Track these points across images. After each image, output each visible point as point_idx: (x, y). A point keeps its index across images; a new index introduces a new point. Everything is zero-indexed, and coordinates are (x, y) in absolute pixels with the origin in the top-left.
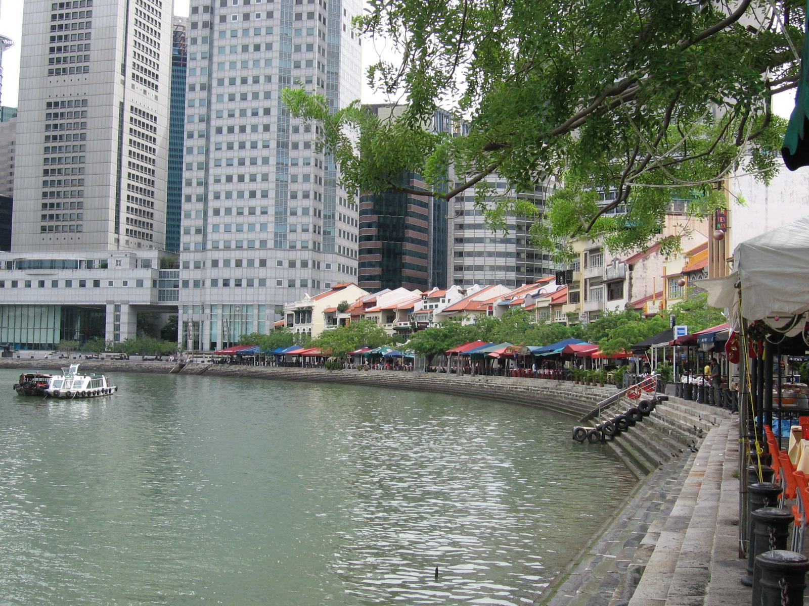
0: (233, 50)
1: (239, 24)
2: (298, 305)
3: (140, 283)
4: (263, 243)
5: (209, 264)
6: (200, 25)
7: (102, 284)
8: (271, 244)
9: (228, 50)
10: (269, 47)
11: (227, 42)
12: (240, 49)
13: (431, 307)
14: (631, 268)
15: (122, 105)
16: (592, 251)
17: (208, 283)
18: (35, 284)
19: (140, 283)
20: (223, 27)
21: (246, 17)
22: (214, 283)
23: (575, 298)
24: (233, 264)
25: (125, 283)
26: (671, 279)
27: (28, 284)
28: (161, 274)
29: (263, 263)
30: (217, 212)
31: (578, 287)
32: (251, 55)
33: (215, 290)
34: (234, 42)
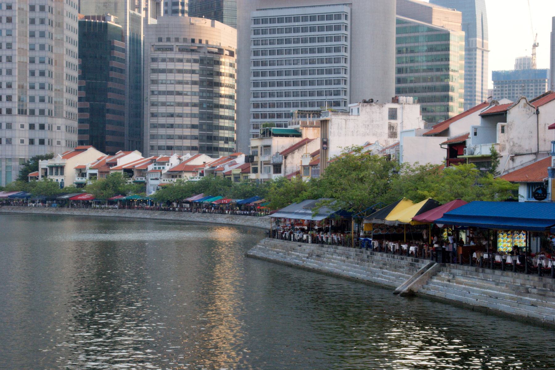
2: (50, 162)
4: (9, 111)
8: (15, 111)
13: (159, 168)
14: (286, 158)
16: (265, 146)
23: (255, 171)
26: (304, 167)
31: (257, 164)
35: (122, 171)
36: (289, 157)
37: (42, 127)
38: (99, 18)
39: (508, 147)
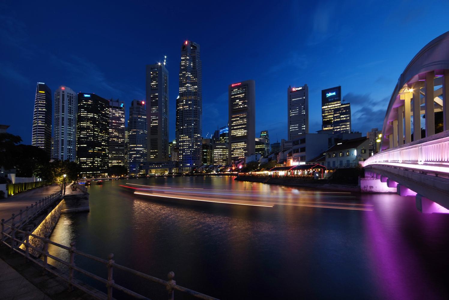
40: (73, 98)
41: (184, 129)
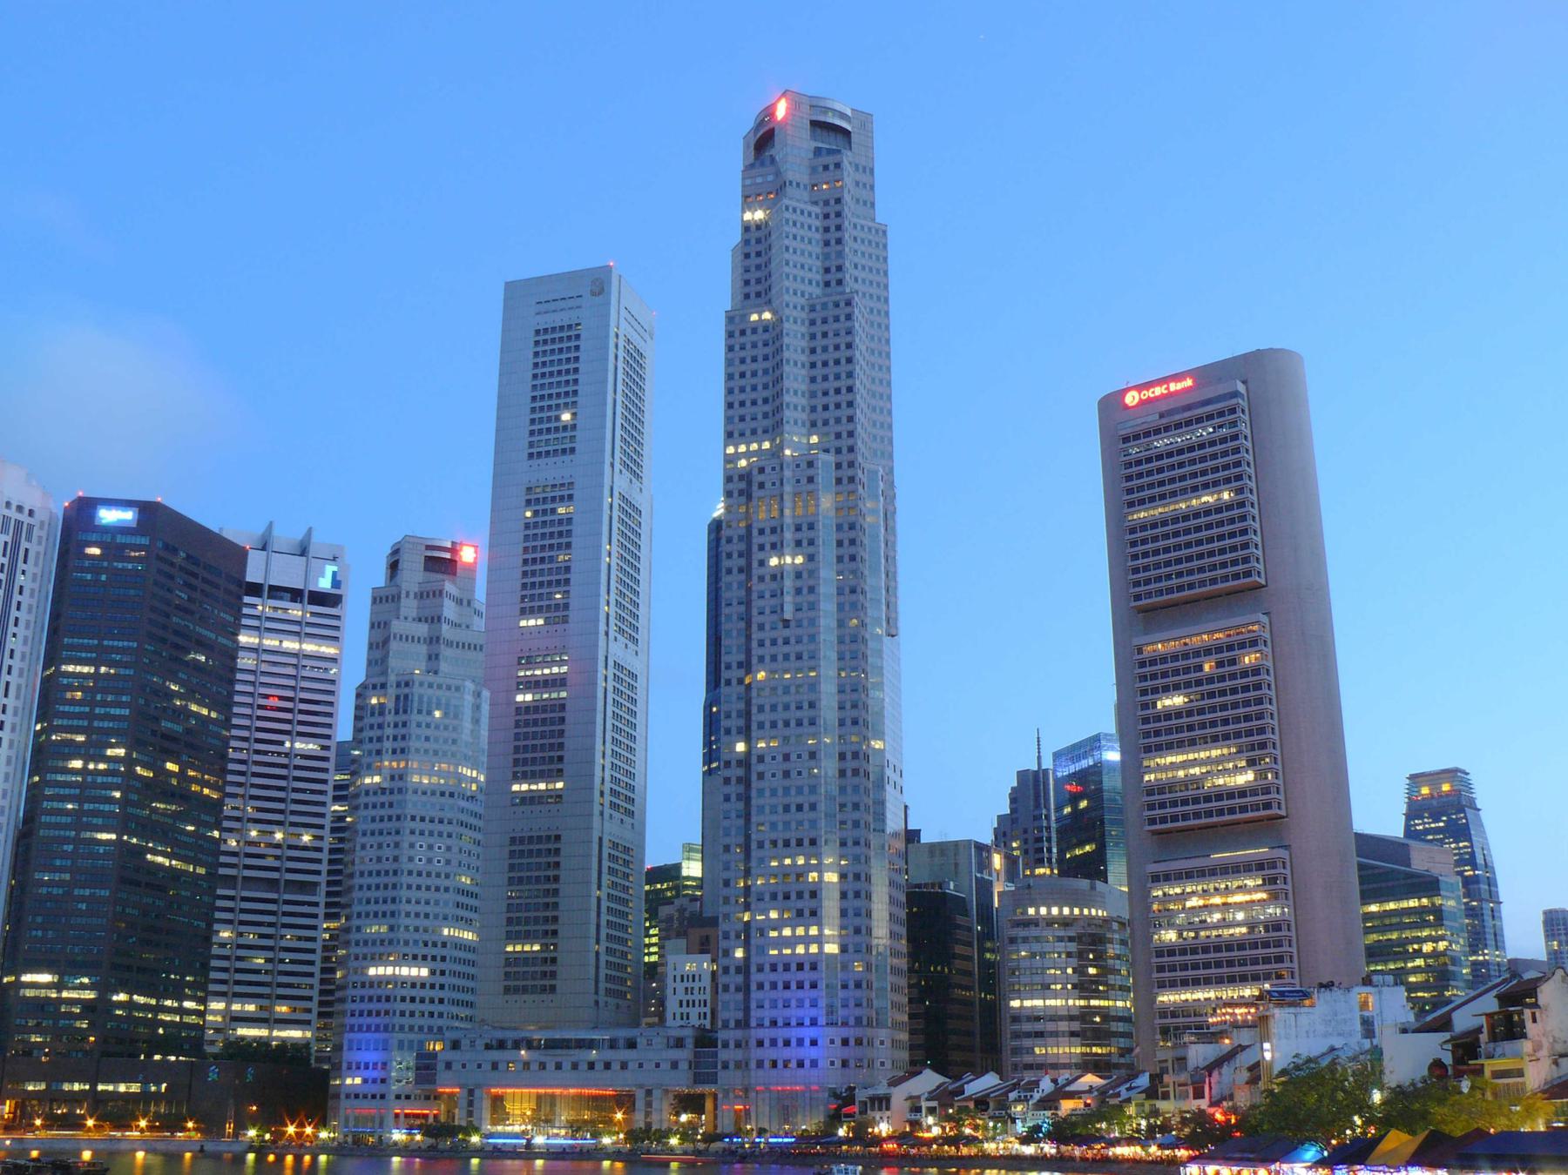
0: (774, 811)
1: (778, 782)
2: (871, 1092)
3: (675, 1065)
4: (814, 1023)
5: (753, 1043)
6: (733, 781)
7: (630, 1065)
9: (767, 810)
10: (813, 807)
11: (767, 801)
12: (780, 809)
15: (601, 839)
17: (753, 1065)
18: (551, 1066)
19: (675, 1065)
20: (762, 784)
21: (787, 774)
22: (760, 1064)
23: (1166, 1096)
24: (780, 1043)
25: (658, 1065)
27: (543, 1066)
28: (696, 1055)
29: (814, 1043)
30: (760, 986)
32: (794, 815)
33: (760, 1072)
34: (774, 801)
35: (971, 1105)
36: (1215, 1073)
37: (859, 1042)
38: (933, 885)
39: (1546, 1045)
40: (35, 539)
41: (761, 759)
